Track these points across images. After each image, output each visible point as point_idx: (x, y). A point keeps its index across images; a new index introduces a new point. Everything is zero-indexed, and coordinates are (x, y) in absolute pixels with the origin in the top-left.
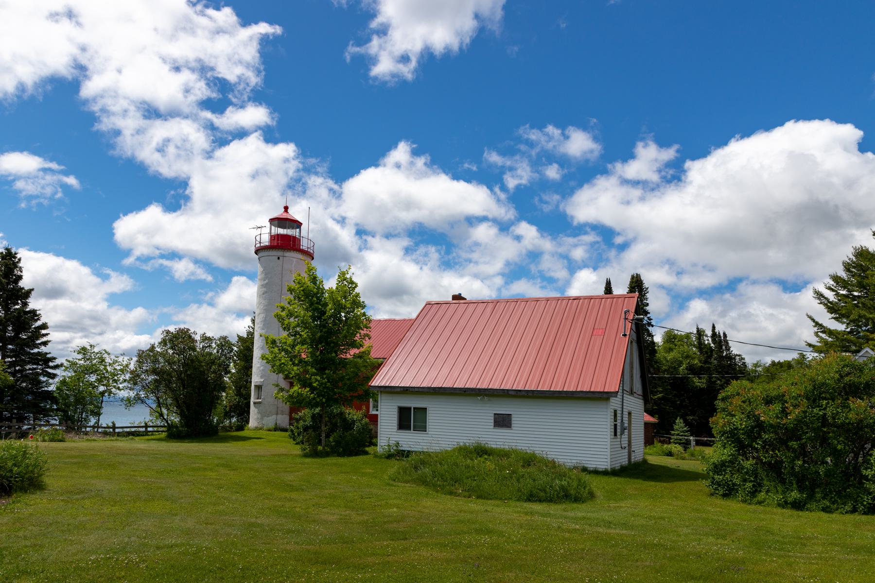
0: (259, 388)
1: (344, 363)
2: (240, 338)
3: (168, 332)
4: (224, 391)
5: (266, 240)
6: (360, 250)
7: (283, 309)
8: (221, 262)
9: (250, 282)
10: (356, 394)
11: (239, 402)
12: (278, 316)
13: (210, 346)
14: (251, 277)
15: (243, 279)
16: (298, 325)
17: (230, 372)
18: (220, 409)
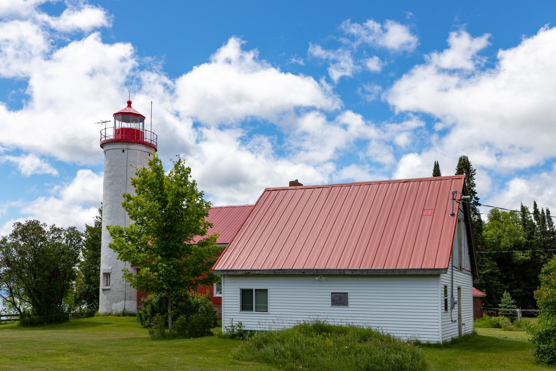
0: (107, 275)
1: (188, 250)
2: (89, 228)
3: (19, 224)
4: (74, 280)
5: (111, 134)
6: (197, 142)
7: (129, 198)
8: (63, 156)
9: (95, 175)
10: (200, 278)
11: (89, 289)
12: (124, 205)
13: (59, 237)
14: (95, 170)
15: (88, 172)
16: (145, 215)
17: (79, 261)
18: (71, 297)
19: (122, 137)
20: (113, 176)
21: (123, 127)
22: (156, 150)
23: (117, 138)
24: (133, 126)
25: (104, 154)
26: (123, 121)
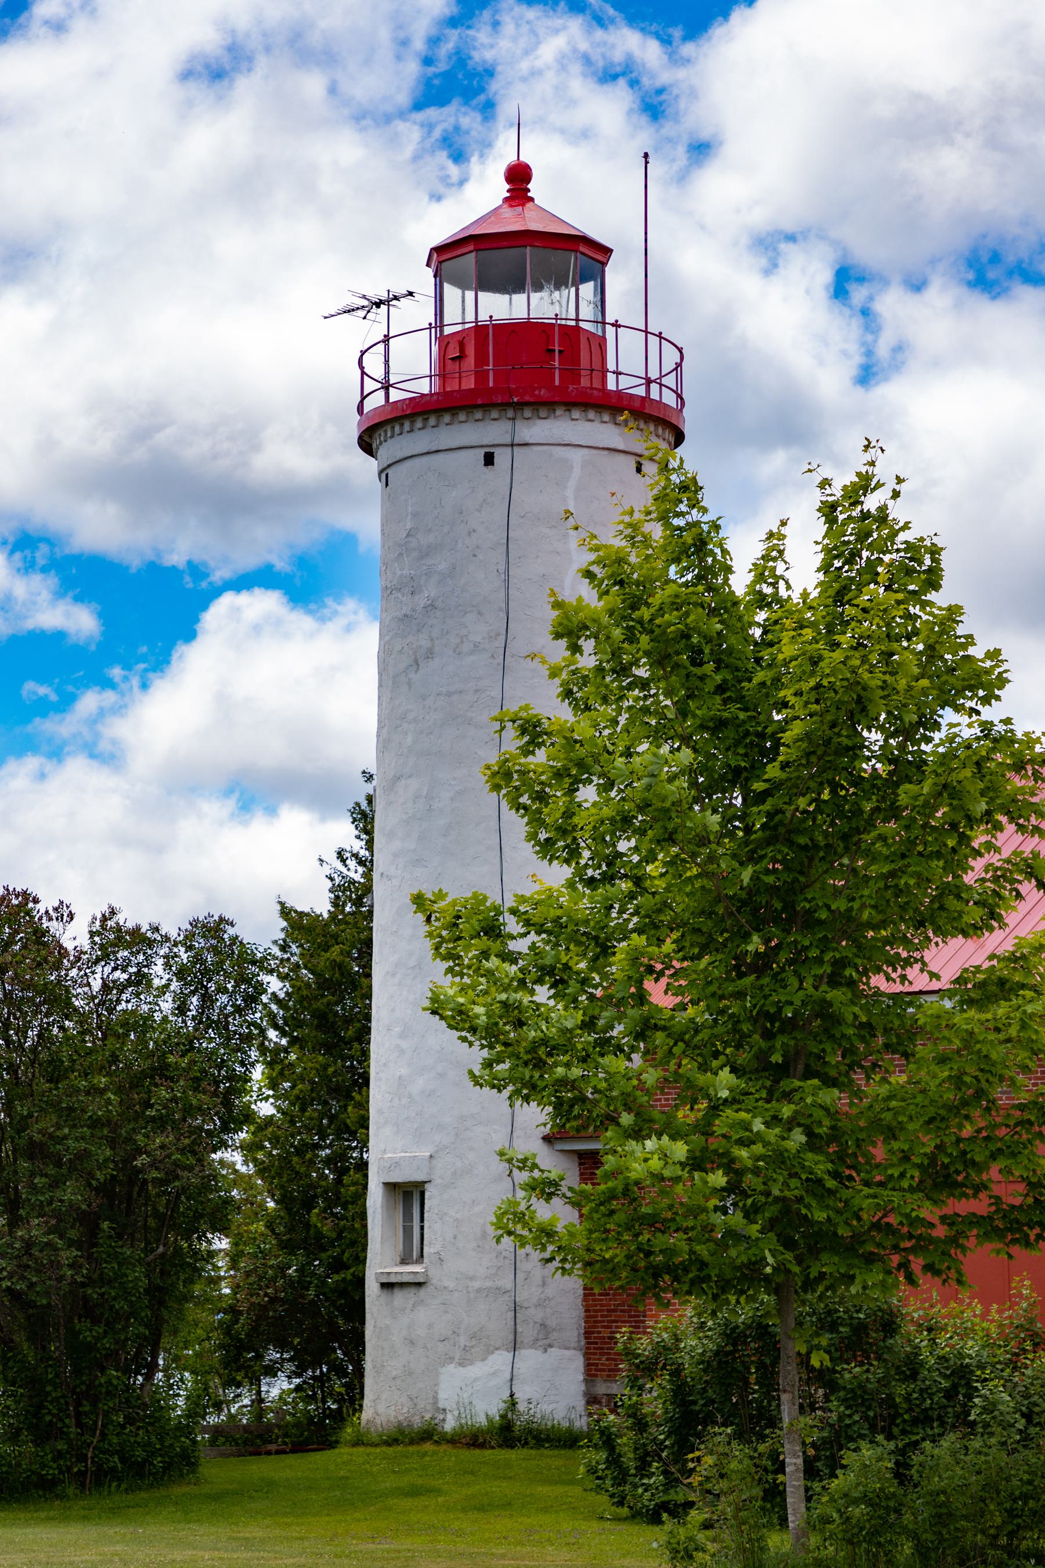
0: (408, 1195)
1: (897, 1031)
2: (298, 924)
4: (223, 1229)
5: (415, 367)
6: (867, 375)
7: (533, 732)
8: (100, 527)
9: (301, 621)
10: (980, 1206)
11: (300, 1284)
12: (502, 777)
13: (140, 980)
16: (623, 822)
17: (248, 1117)
18: (199, 1330)
19: (481, 376)
20: (431, 607)
21: (483, 316)
22: (679, 438)
23: (452, 386)
24: (542, 305)
25: (379, 486)
26: (485, 283)
